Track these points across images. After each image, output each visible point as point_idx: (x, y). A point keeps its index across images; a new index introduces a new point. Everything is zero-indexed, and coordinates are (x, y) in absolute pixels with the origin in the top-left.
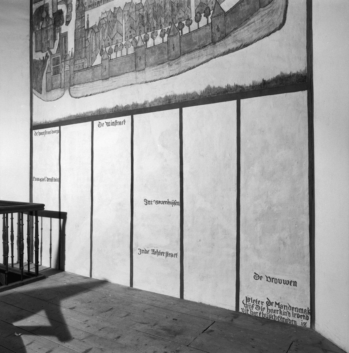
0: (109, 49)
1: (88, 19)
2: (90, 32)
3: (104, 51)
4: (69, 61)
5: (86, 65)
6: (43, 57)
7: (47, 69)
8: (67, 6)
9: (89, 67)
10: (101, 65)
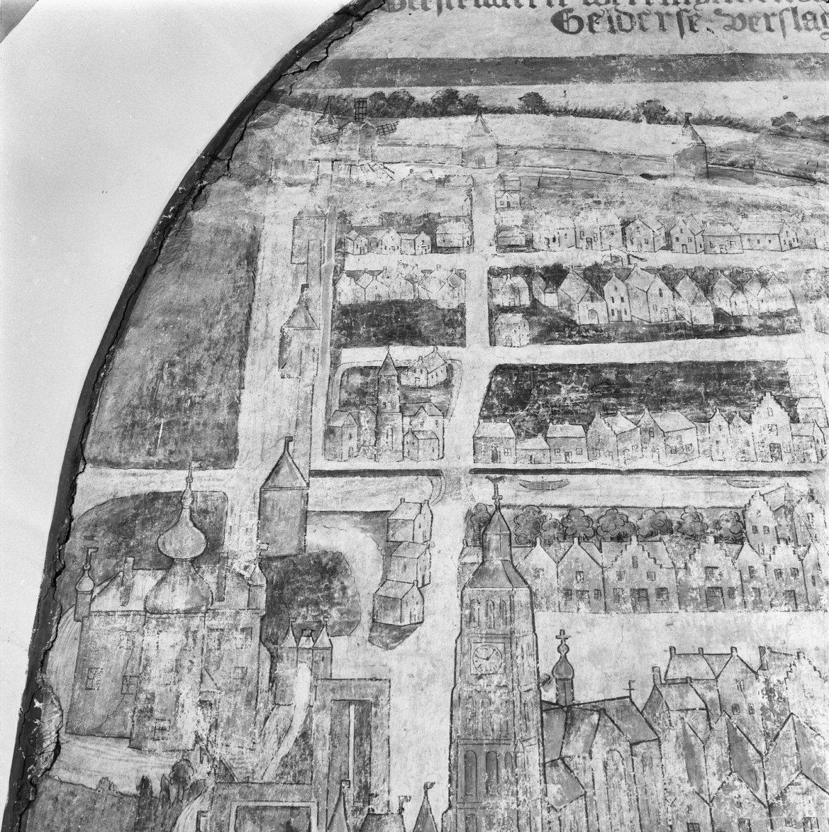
1: (563, 648)
2: (585, 728)
6: (145, 783)
8: (390, 549)
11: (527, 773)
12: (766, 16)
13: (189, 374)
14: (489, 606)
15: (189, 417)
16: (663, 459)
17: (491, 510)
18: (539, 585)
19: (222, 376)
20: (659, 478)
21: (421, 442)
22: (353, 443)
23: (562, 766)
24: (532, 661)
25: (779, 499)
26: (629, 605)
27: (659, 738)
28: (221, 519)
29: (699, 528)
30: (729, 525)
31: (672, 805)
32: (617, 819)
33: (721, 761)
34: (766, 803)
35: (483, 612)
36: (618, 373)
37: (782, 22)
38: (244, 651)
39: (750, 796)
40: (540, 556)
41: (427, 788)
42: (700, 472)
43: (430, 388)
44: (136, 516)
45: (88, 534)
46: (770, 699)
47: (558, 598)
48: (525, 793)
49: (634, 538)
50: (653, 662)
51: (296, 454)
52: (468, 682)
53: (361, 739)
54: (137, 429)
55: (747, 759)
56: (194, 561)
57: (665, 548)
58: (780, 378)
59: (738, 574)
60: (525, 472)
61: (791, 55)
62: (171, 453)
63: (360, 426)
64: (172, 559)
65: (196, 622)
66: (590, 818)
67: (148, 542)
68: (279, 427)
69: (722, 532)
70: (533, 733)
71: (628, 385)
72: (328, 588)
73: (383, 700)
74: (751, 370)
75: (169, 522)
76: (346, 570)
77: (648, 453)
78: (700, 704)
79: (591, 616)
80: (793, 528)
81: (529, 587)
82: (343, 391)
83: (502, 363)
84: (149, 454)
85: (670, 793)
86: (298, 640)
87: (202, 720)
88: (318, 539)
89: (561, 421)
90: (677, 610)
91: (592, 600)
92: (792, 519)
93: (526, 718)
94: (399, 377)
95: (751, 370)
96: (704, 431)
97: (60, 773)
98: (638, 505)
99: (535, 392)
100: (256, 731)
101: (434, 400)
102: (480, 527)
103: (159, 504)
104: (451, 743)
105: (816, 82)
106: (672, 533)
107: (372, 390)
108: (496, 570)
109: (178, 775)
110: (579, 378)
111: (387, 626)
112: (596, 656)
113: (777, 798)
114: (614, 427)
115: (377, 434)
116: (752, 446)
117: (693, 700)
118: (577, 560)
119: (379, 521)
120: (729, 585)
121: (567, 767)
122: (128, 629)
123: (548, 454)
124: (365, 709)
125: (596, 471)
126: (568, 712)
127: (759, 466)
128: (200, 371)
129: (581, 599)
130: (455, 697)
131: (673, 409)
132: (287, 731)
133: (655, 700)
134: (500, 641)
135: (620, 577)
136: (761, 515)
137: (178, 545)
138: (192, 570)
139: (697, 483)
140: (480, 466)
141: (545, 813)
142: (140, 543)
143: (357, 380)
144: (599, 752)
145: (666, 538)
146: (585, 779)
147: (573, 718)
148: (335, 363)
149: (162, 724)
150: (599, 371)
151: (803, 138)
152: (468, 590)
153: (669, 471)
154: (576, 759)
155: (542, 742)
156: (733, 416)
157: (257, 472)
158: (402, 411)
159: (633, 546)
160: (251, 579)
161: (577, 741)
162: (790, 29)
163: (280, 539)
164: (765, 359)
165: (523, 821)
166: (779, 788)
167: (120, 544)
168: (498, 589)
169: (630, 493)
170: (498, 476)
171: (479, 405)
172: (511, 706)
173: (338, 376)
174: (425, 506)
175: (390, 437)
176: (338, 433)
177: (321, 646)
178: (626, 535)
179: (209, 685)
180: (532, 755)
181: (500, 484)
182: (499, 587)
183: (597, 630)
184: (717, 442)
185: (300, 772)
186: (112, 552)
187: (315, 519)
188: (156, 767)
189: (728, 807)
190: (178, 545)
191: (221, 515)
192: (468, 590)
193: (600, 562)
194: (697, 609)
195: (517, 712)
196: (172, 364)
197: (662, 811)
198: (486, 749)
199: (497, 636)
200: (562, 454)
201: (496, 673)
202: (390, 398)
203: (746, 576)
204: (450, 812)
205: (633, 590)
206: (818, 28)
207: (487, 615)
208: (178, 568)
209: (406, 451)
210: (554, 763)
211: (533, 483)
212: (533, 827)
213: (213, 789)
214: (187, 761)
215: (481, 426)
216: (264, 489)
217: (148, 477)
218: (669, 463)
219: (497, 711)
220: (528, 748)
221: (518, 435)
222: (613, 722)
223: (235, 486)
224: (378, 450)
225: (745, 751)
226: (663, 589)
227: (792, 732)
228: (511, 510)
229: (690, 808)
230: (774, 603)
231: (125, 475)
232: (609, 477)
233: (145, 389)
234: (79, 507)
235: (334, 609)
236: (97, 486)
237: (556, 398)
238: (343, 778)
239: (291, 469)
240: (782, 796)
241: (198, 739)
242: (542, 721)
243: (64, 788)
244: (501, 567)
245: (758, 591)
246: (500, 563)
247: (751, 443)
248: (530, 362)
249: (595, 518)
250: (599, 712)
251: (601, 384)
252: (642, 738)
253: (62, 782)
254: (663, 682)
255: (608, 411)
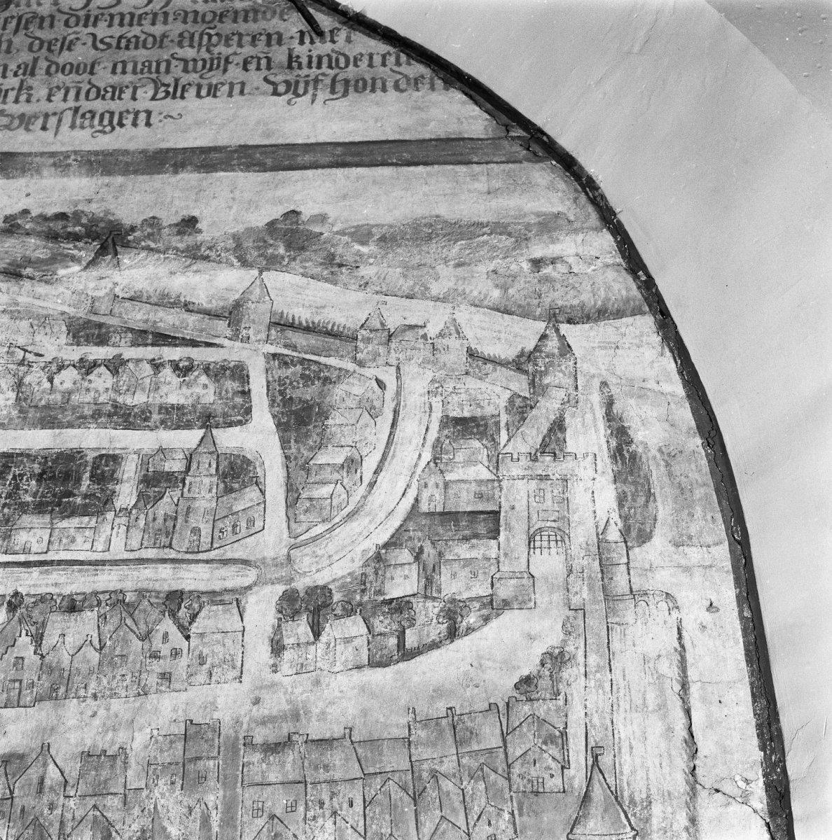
12: (47, 116)
37: (60, 121)
61: (53, 153)
105: (65, 179)
151: (28, 234)
162: (65, 128)
206: (92, 126)
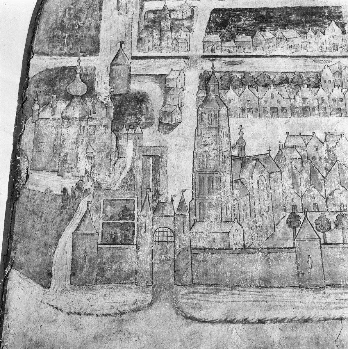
0: (320, 218)
1: (241, 133)
2: (250, 167)
3: (302, 220)
4: (172, 218)
5: (237, 240)
6: (65, 190)
7: (80, 224)
8: (167, 91)
9: (251, 248)
10: (293, 250)
11: (225, 185)
13: (77, 13)
14: (210, 115)
15: (78, 33)
16: (286, 51)
17: (210, 74)
18: (230, 106)
19: (92, 14)
20: (284, 59)
21: (180, 44)
22: (150, 44)
23: (240, 182)
24: (228, 139)
25: (336, 68)
26: (270, 115)
27: (281, 171)
28: (94, 78)
29: (300, 81)
30: (314, 80)
31: (286, 198)
32: (263, 204)
33: (307, 180)
34: (325, 197)
35: (207, 118)
36: (267, 12)
38: (104, 135)
39: (319, 194)
40: (231, 94)
41: (183, 191)
42: (302, 56)
43: (184, 19)
44: (56, 77)
45: (36, 85)
46: (328, 154)
47: (239, 111)
48: (224, 193)
49: (272, 85)
50: (279, 139)
51: (125, 50)
52: (200, 148)
53: (155, 172)
54: (55, 39)
55: (318, 179)
56: (82, 96)
57: (285, 90)
58: (338, 14)
59: (317, 101)
60: (225, 57)
62: (71, 49)
63: (153, 37)
64: (73, 96)
65: (84, 123)
66: (251, 203)
67: (62, 88)
68: (118, 37)
69: (310, 83)
70: (228, 169)
71: (271, 18)
72: (140, 108)
73: (164, 155)
74: (326, 10)
75: (71, 80)
76: (148, 100)
77: (279, 48)
78: (299, 156)
79: (253, 119)
80: (341, 81)
81: (227, 107)
82: (145, 21)
83: (216, 8)
84: (61, 50)
85: (285, 193)
86: (127, 130)
87: (88, 164)
88: (135, 87)
89: (241, 34)
90: (290, 116)
91: (254, 112)
92: (341, 77)
93: (225, 162)
94: (170, 15)
95: (326, 10)
96: (304, 38)
97: (29, 186)
98: (275, 71)
99: (230, 21)
100: (111, 168)
101: (185, 25)
102: (206, 81)
103: (66, 72)
104: (193, 173)
106: (289, 83)
107: (158, 20)
108: (213, 99)
109: (78, 187)
110: (250, 15)
111: (166, 124)
112: (255, 137)
113: (330, 195)
114: (265, 36)
115: (161, 40)
116: (325, 45)
117: (296, 155)
118: (247, 95)
119: (161, 79)
120: (313, 106)
121: (242, 183)
122: (55, 126)
123: (235, 49)
124: (157, 159)
125: (256, 56)
126: (243, 160)
127: (327, 54)
128: (82, 12)
129: (249, 112)
130: (195, 154)
131: (291, 28)
132: (124, 168)
133: (280, 154)
134: (214, 130)
135: (266, 103)
136: (328, 75)
137: (75, 89)
138: (82, 100)
139: (300, 62)
140: (206, 54)
141: (232, 201)
142: (59, 89)
143: (151, 16)
144: (256, 177)
145: (286, 85)
146: (250, 187)
147: (245, 162)
148: (142, 9)
149: (71, 166)
150: (259, 11)
152: (200, 108)
153: (288, 56)
154: (246, 179)
155: (231, 172)
156: (317, 31)
157: (108, 57)
158: (171, 30)
159: (272, 89)
160: (107, 104)
161: (246, 172)
163: (119, 87)
164: (332, 5)
165: (223, 205)
166: (331, 191)
167: (50, 89)
168: (213, 108)
169: (271, 66)
170: (214, 58)
171: (205, 27)
172: (219, 158)
173: (143, 14)
174: (182, 72)
175: (166, 42)
176: (144, 40)
177: (137, 133)
178: (269, 84)
179: (90, 150)
180: (227, 178)
181: (214, 62)
182: (214, 107)
183: (255, 126)
184: (310, 43)
185: (130, 185)
186: (47, 93)
187: (134, 78)
188: (70, 184)
189: (309, 199)
190: (75, 89)
191: (93, 77)
192: (200, 108)
193: (257, 96)
194: (299, 116)
195: (221, 159)
196: (70, 9)
197: (281, 200)
198: (208, 175)
199: (213, 128)
200: (242, 49)
201: (212, 144)
202: (166, 24)
203: (320, 102)
204: (193, 201)
205: (271, 108)
207: (208, 119)
208: (75, 100)
209: (173, 48)
210: (236, 181)
211: (229, 62)
212: (227, 207)
213: (94, 192)
214: (82, 181)
215: (206, 36)
216: (112, 65)
217: (61, 60)
218: (288, 52)
219: (213, 159)
220: (225, 175)
221: (222, 40)
222: (262, 164)
223: (99, 63)
224: (161, 47)
225: (317, 176)
226: (284, 108)
227: (337, 168)
228: (219, 74)
229: (293, 199)
230: (331, 113)
231: (51, 59)
232: (262, 59)
233: (58, 21)
234: (32, 73)
235: (143, 117)
236: (40, 64)
237: (239, 24)
238: (148, 187)
239: (123, 56)
240: (332, 194)
241: (86, 172)
242: (232, 164)
243: (31, 192)
244: (215, 98)
245: (325, 108)
246: (214, 96)
247: (325, 43)
248: (228, 7)
249: (256, 77)
250: (256, 160)
251: (259, 17)
252: (274, 171)
253: (30, 190)
254: (284, 147)
255: (262, 29)
